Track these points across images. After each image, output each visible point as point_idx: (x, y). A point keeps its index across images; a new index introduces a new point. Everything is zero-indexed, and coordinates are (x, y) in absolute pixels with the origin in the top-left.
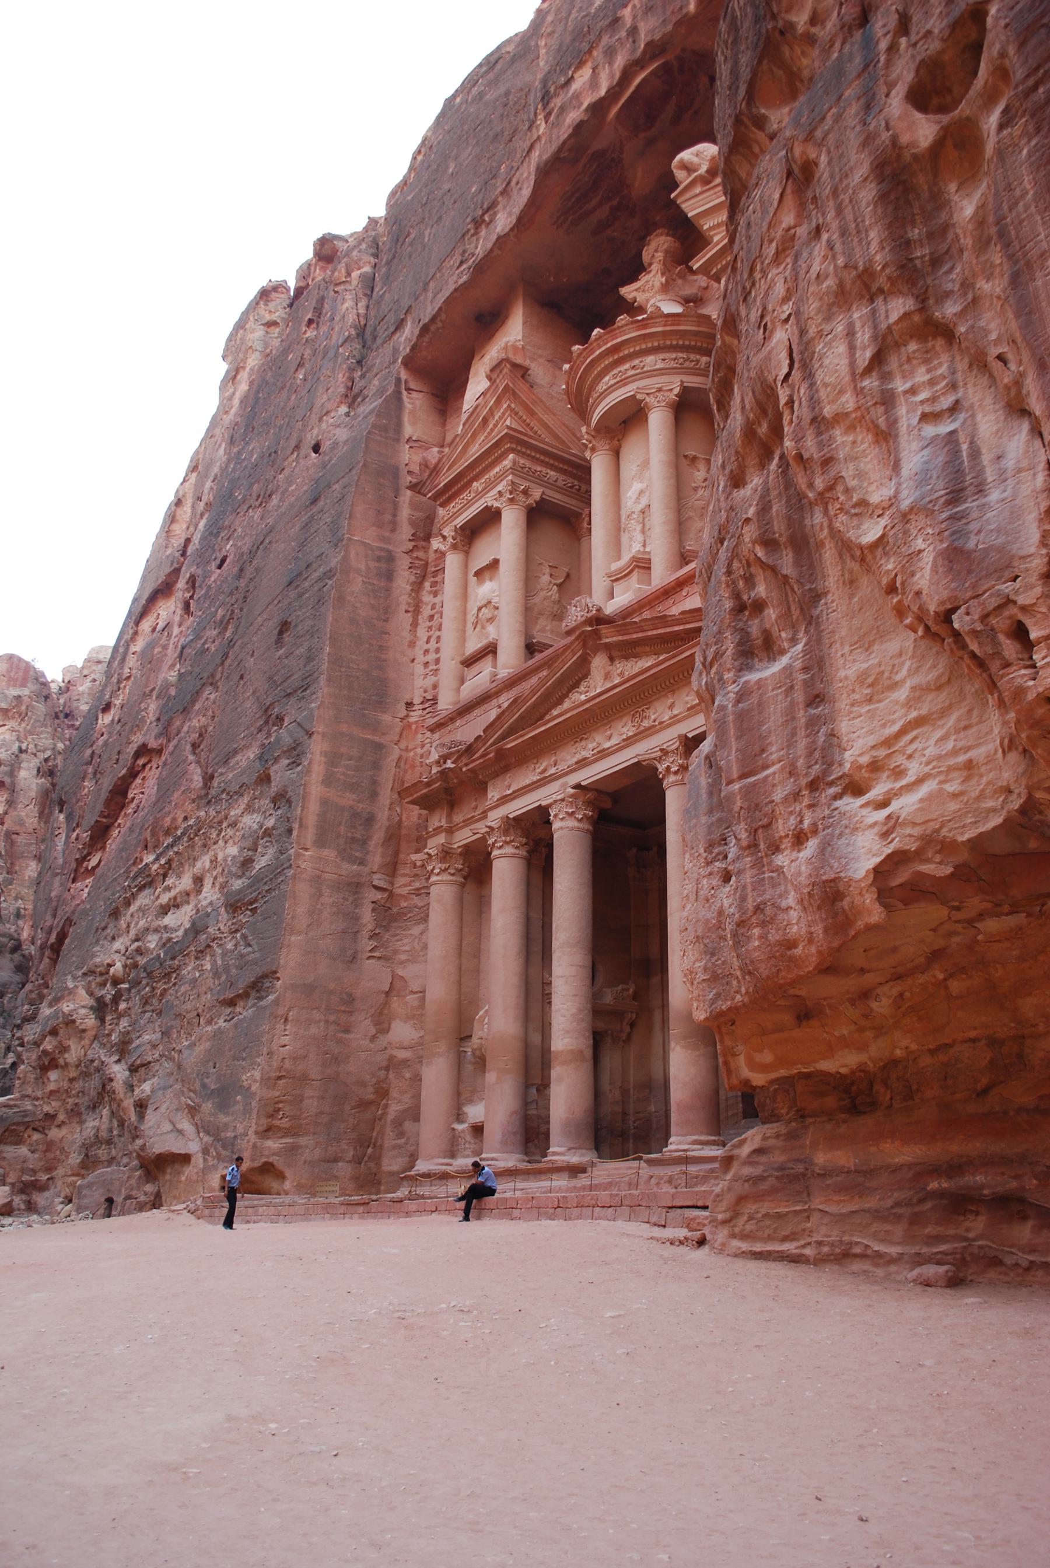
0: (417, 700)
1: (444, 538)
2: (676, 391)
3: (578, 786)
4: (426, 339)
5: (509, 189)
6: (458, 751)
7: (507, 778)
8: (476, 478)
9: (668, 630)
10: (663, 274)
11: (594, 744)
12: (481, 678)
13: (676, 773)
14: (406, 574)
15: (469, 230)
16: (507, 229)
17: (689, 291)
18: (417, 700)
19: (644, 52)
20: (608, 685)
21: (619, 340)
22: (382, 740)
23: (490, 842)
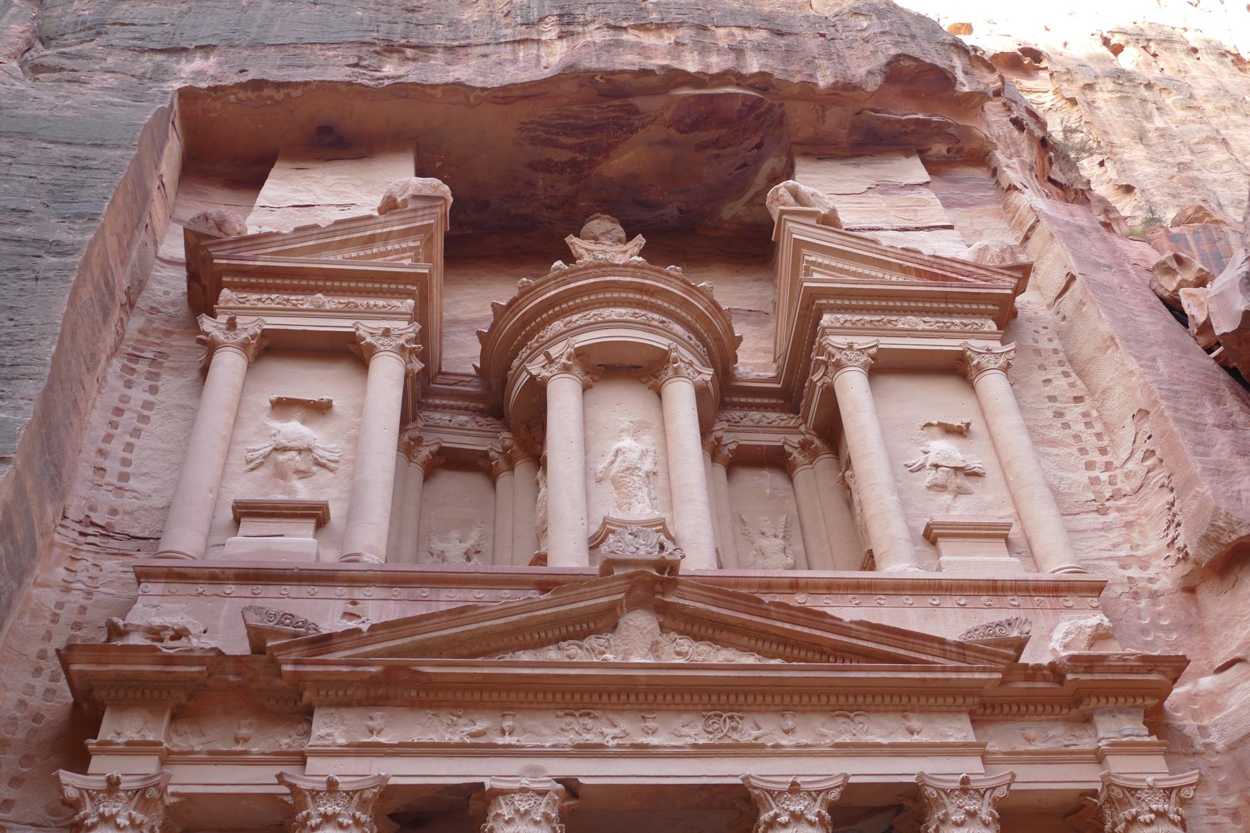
1: (232, 325)
3: (571, 787)
4: (242, 95)
5: (462, 51)
6: (295, 635)
7: (378, 718)
8: (327, 291)
9: (818, 633)
11: (616, 731)
12: (296, 544)
14: (113, 329)
15: (374, 44)
16: (478, 85)
18: (71, 514)
19: (753, 75)
20: (651, 660)
22: (40, 543)
23: (330, 811)
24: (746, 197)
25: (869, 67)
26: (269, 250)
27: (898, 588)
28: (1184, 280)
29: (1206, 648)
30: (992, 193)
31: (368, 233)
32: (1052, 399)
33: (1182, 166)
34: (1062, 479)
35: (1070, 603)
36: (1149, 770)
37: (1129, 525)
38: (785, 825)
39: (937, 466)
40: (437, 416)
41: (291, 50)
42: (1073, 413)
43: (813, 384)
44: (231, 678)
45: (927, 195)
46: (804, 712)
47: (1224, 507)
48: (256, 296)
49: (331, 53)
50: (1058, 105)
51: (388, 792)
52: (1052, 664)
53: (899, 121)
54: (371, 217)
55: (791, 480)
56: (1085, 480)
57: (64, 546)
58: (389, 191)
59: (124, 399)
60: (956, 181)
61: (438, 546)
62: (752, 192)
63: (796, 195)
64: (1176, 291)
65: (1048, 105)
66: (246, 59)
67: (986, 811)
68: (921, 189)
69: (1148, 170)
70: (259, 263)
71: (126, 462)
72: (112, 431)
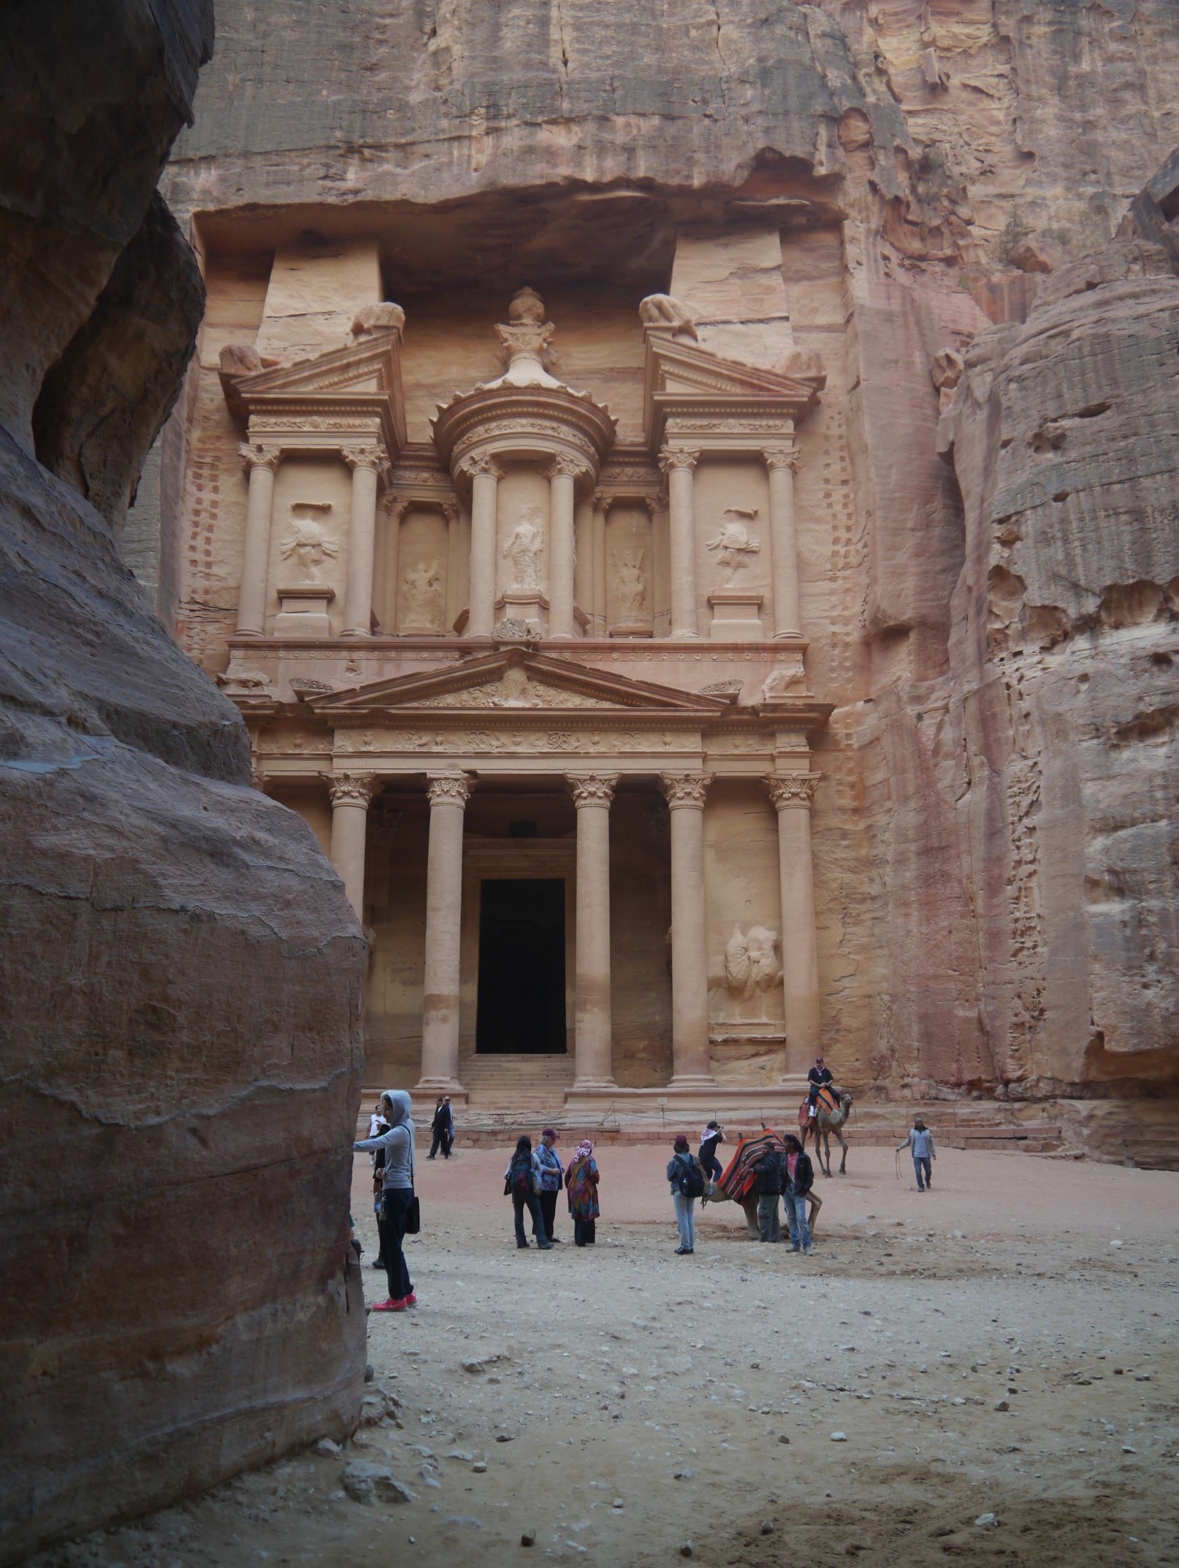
0: (185, 598)
1: (260, 449)
2: (584, 470)
3: (472, 773)
4: (241, 214)
5: (409, 148)
7: (369, 735)
10: (545, 340)
12: (314, 619)
13: (600, 798)
15: (338, 147)
16: (421, 200)
17: (546, 361)
18: (185, 598)
21: (551, 400)
23: (346, 788)
25: (738, 160)
26: (278, 383)
28: (948, 378)
30: (836, 264)
31: (345, 362)
32: (827, 481)
33: (1089, 125)
34: (814, 552)
35: (782, 658)
36: (798, 769)
37: (847, 591)
38: (585, 798)
39: (726, 548)
40: (407, 474)
41: (275, 159)
42: (839, 493)
43: (659, 468)
44: (289, 715)
45: (776, 280)
46: (606, 731)
47: (884, 605)
48: (273, 420)
49: (305, 161)
50: (994, 41)
51: (378, 776)
53: (763, 207)
54: (345, 348)
55: (650, 519)
57: (183, 621)
58: (357, 318)
59: (199, 501)
60: (810, 250)
61: (412, 576)
63: (659, 307)
64: (943, 384)
65: (984, 40)
66: (240, 174)
69: (1053, 132)
70: (272, 396)
71: (208, 553)
72: (196, 530)
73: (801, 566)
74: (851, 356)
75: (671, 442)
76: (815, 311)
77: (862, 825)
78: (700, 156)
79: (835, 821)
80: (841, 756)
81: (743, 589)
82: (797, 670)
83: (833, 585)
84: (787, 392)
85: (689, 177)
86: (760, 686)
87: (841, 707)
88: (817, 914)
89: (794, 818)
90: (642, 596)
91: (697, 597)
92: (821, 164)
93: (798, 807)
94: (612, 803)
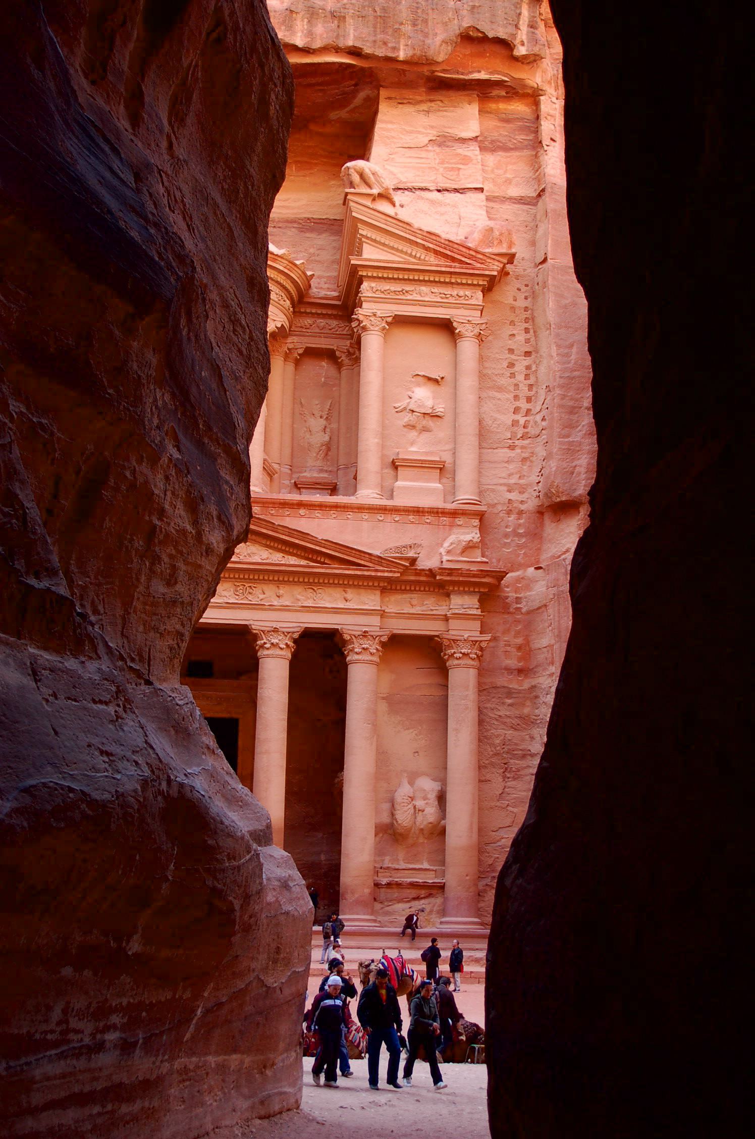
24: (348, 109)
27: (361, 508)
29: (539, 549)
32: (511, 351)
34: (495, 420)
37: (524, 460)
38: (268, 649)
39: (413, 411)
42: (521, 364)
45: (472, 151)
52: (430, 570)
53: (465, 80)
56: (510, 423)
60: (507, 121)
62: (352, 106)
67: (374, 647)
68: (471, 143)
73: (483, 433)
74: (541, 231)
75: (365, 305)
76: (508, 182)
77: (526, 685)
78: (407, 28)
79: (502, 680)
80: (510, 618)
81: (427, 453)
82: (474, 535)
83: (512, 454)
84: (479, 265)
85: (395, 49)
86: (441, 549)
87: (512, 571)
88: (480, 767)
89: (463, 679)
90: (328, 447)
91: (383, 457)
92: (523, 45)
93: (468, 667)
94: (294, 655)
